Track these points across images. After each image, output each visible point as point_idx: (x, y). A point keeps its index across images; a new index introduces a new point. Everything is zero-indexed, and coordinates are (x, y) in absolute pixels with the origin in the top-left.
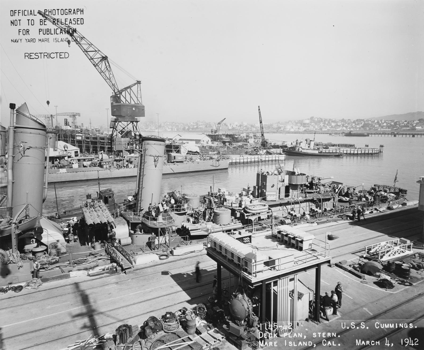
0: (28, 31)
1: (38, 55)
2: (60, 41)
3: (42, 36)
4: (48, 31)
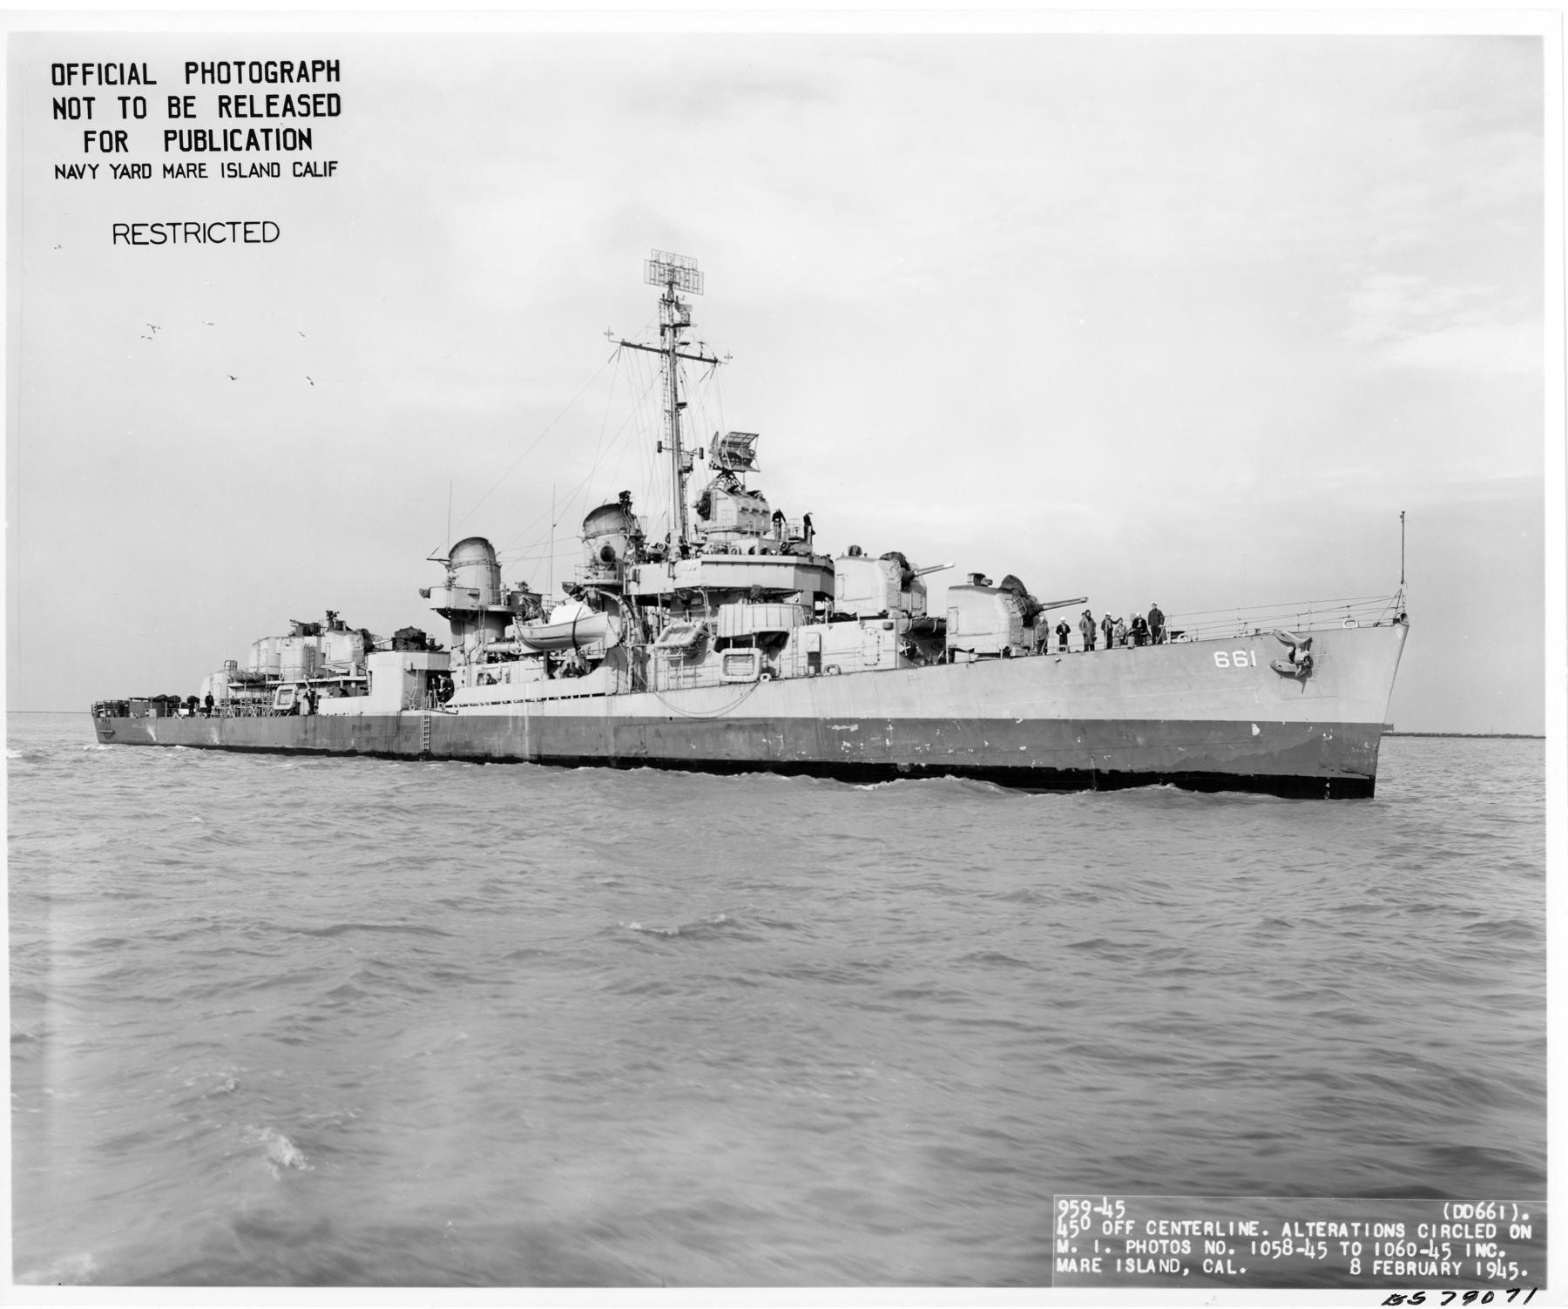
0: (120, 139)
1: (161, 232)
2: (246, 172)
3: (176, 157)
4: (200, 139)
